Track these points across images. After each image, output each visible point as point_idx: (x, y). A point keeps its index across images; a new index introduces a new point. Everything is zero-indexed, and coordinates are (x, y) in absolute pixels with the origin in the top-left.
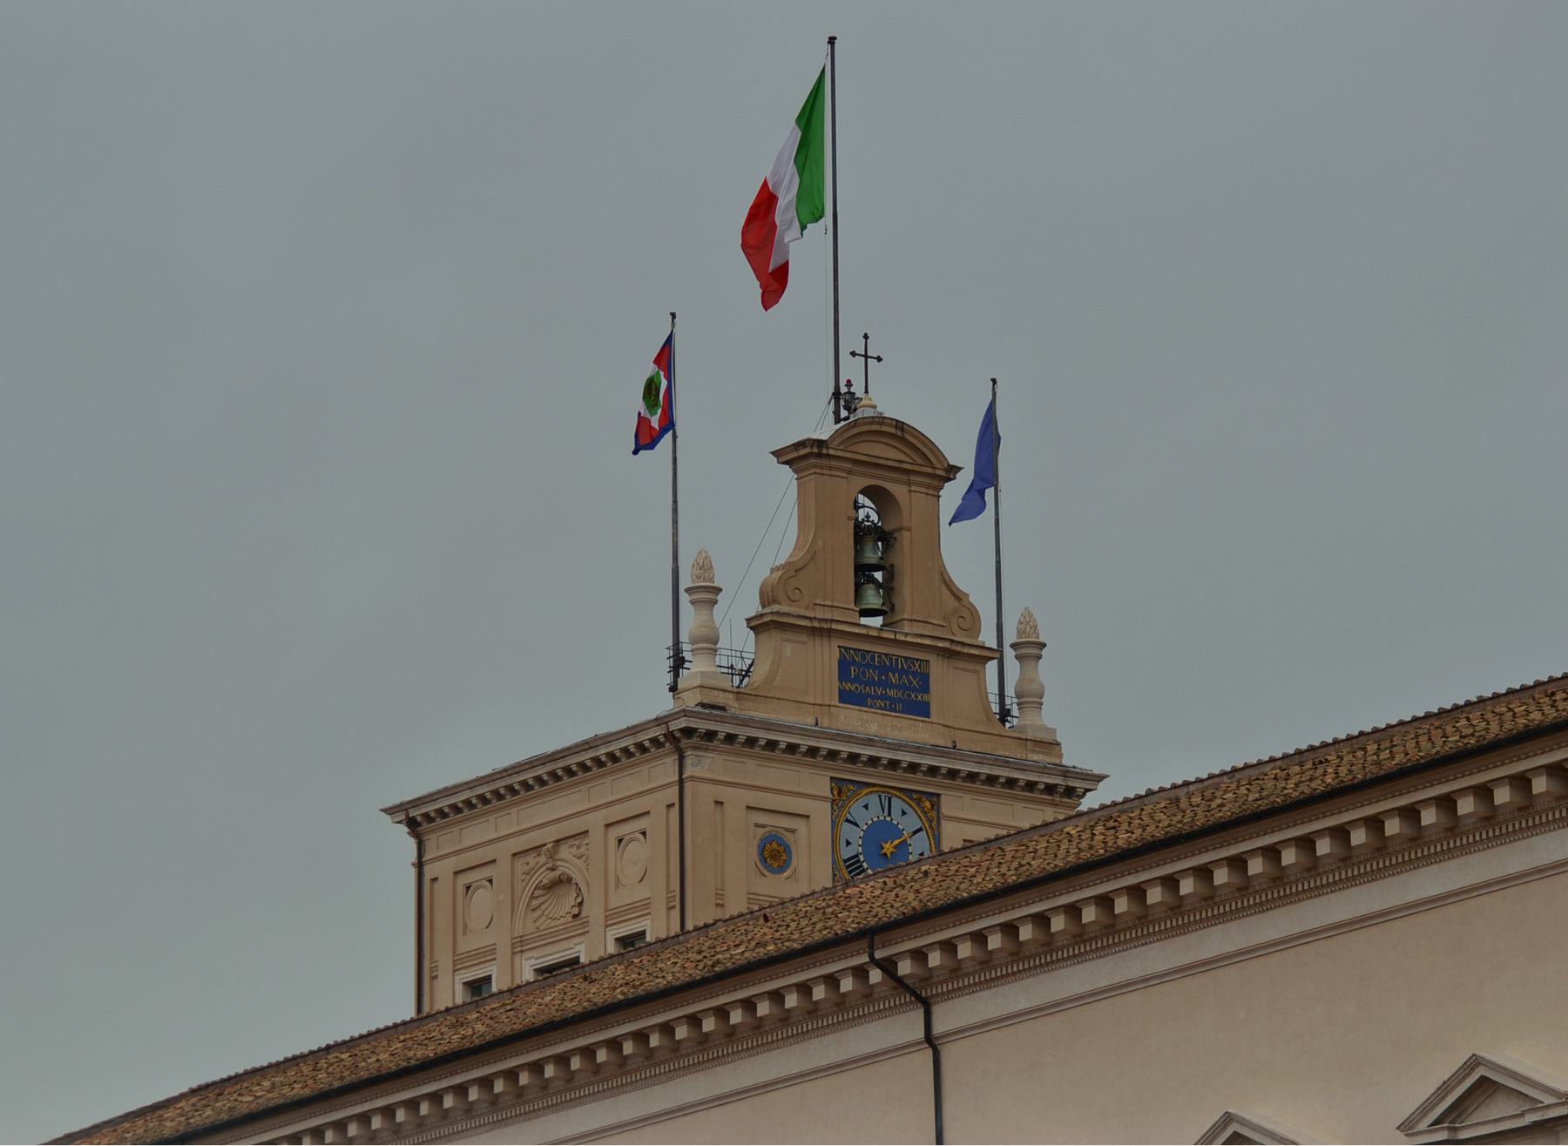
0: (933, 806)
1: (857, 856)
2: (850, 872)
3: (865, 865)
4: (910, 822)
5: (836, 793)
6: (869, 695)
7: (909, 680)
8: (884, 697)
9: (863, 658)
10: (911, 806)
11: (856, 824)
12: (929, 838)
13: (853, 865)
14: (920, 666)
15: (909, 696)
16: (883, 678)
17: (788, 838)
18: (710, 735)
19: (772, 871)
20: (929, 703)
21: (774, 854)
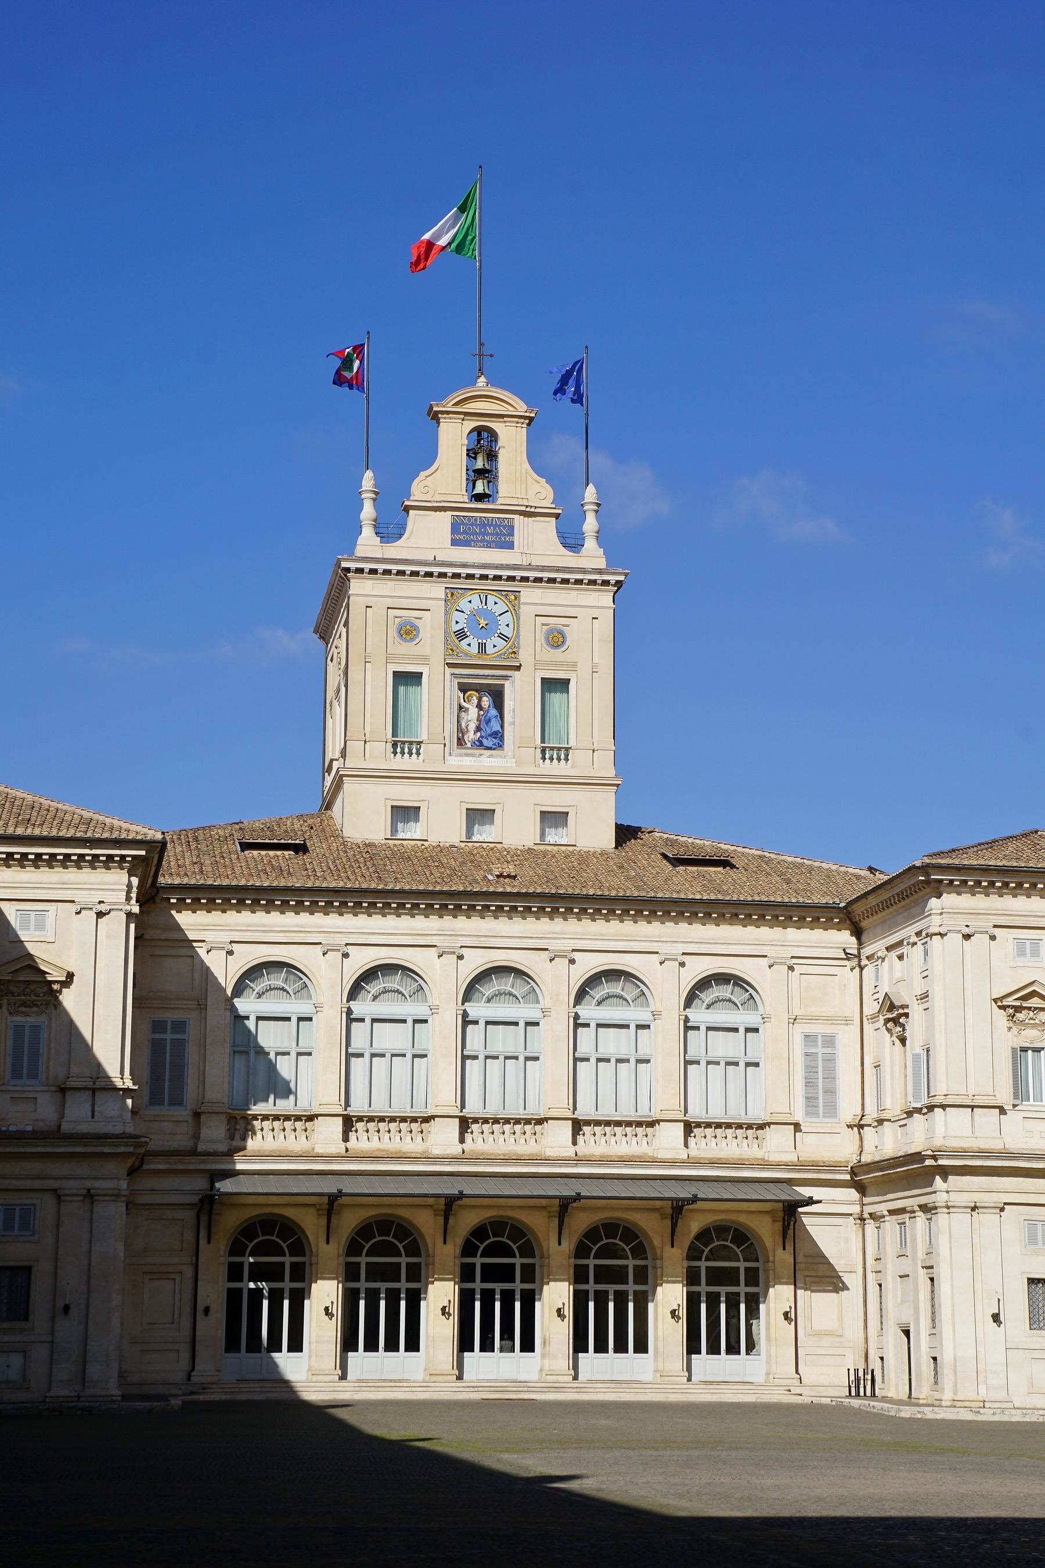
0: (516, 598)
1: (463, 629)
2: (458, 638)
3: (468, 634)
4: (502, 607)
5: (449, 596)
6: (472, 540)
7: (500, 529)
8: (481, 541)
9: (469, 520)
10: (501, 599)
11: (463, 612)
12: (513, 615)
13: (461, 635)
14: (508, 522)
15: (500, 538)
16: (483, 530)
17: (416, 622)
18: (360, 571)
19: (405, 640)
20: (513, 542)
21: (408, 632)
